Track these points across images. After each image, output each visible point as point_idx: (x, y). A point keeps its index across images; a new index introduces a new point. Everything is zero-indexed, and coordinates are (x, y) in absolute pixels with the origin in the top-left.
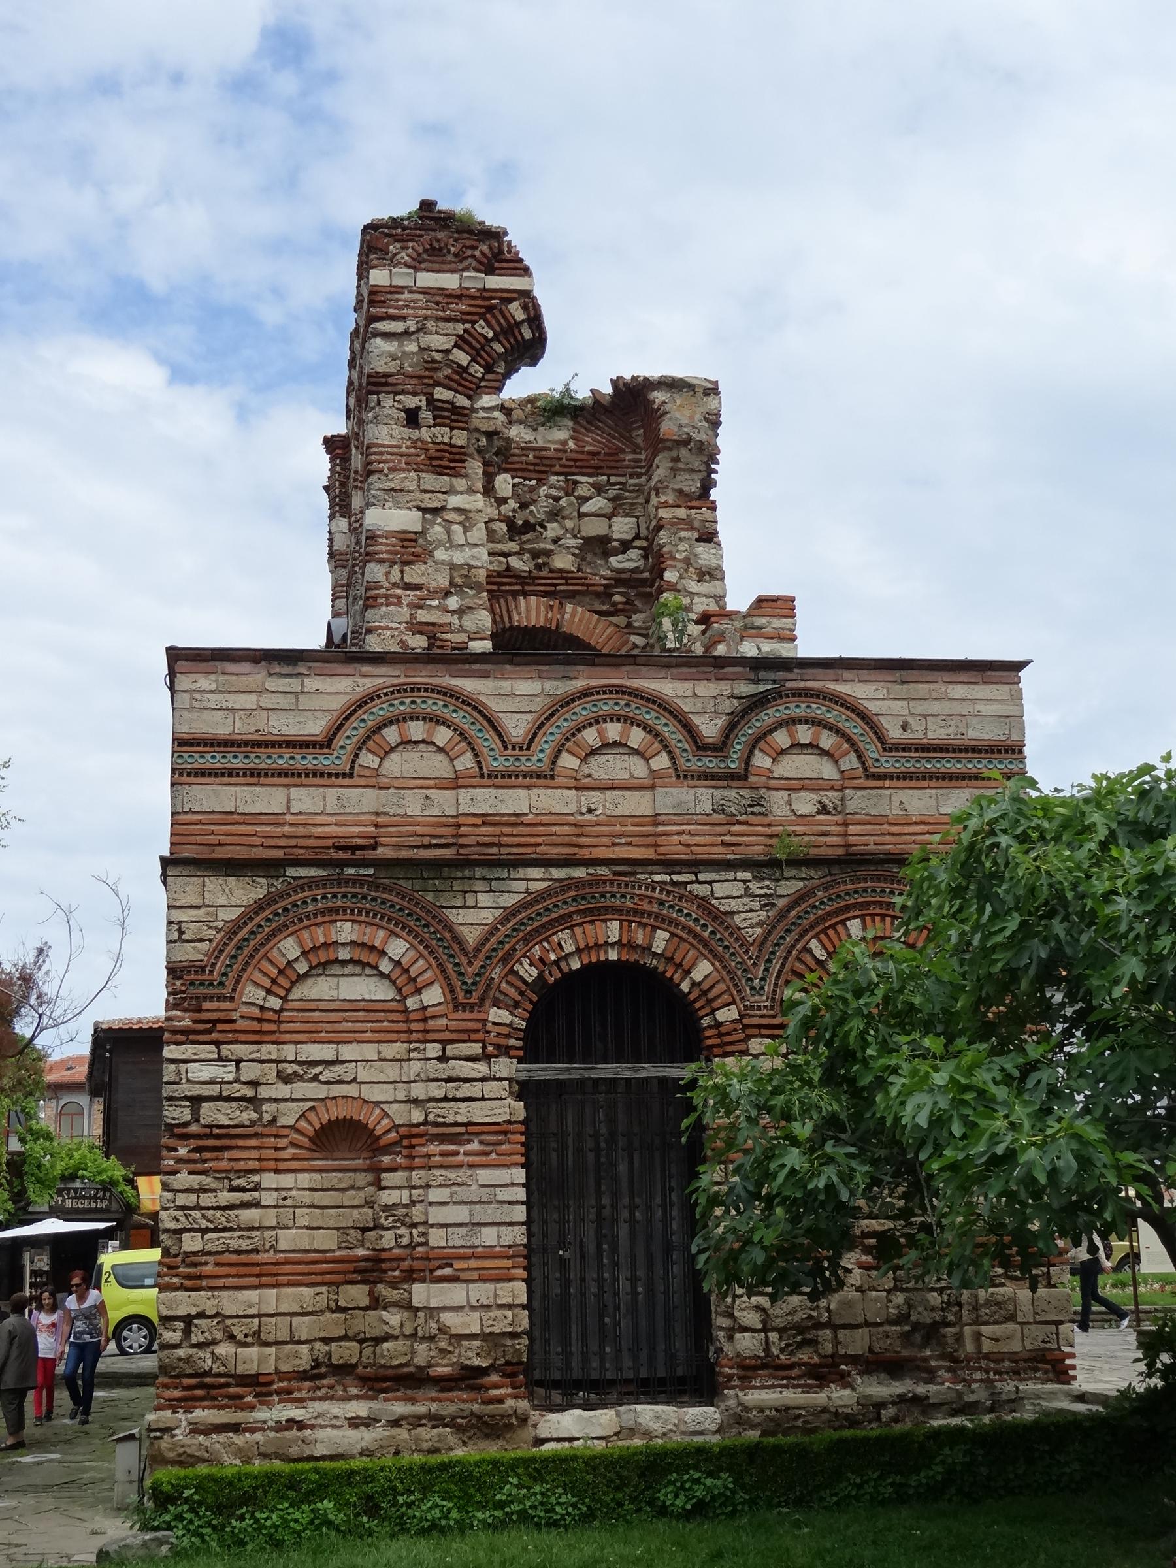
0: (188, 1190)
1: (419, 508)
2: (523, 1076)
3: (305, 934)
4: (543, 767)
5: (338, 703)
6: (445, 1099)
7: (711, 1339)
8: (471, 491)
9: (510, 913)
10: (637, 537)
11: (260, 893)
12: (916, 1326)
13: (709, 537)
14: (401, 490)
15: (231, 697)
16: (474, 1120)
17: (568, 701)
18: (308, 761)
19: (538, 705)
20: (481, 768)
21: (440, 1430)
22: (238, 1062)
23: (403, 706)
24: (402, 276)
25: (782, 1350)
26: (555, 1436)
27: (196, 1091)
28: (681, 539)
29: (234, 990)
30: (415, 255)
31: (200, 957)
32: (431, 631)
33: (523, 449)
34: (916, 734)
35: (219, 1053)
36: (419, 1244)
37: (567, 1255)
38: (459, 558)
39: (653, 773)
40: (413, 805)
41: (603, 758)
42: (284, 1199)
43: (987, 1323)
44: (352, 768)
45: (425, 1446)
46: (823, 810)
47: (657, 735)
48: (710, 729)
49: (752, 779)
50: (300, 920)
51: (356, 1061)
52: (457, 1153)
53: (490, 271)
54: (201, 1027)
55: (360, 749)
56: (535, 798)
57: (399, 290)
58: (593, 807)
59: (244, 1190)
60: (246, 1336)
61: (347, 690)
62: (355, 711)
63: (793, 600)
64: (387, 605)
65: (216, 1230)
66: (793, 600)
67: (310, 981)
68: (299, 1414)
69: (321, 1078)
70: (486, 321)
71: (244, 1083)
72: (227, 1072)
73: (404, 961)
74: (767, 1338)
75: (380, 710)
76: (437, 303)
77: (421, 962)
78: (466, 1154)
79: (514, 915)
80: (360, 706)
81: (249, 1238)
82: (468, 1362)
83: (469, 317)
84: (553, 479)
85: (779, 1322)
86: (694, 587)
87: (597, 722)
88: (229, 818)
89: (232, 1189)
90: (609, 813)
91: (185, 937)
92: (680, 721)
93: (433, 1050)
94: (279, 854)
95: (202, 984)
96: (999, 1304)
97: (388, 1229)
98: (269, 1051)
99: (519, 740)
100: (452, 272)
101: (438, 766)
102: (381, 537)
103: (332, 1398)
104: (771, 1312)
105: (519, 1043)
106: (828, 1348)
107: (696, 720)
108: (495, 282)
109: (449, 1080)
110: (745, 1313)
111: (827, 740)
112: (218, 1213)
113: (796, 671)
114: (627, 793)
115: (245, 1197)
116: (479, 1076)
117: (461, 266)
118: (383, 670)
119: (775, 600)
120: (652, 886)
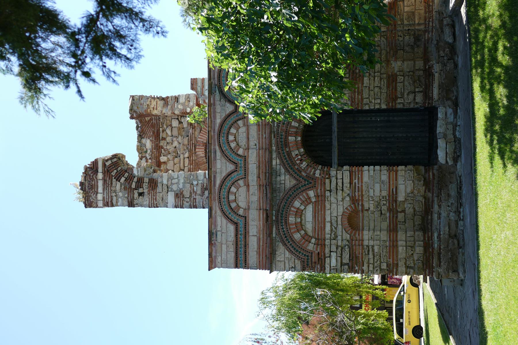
0: (368, 266)
1: (167, 193)
2: (336, 166)
3: (292, 231)
4: (243, 159)
5: (224, 221)
6: (342, 190)
7: (417, 108)
9: (287, 170)
10: (178, 119)
11: (281, 244)
12: (415, 44)
13: (176, 99)
14: (162, 198)
16: (349, 181)
17: (222, 151)
18: (241, 229)
19: (224, 161)
20: (243, 178)
21: (442, 193)
22: (331, 252)
23: (224, 201)
24: (100, 197)
25: (422, 87)
26: (445, 158)
27: (339, 264)
29: (309, 253)
31: (299, 262)
32: (204, 189)
35: (328, 257)
36: (386, 198)
37: (390, 153)
38: (182, 181)
39: (244, 125)
40: (254, 198)
42: (372, 238)
43: (415, 21)
44: (243, 217)
45: (447, 198)
47: (232, 124)
50: (288, 233)
51: (331, 216)
52: (358, 187)
54: (320, 262)
55: (237, 214)
56: (252, 162)
58: (254, 144)
59: (369, 251)
60: (412, 250)
61: (220, 218)
62: (226, 216)
63: (191, 79)
64: (196, 202)
65: (380, 259)
66: (191, 79)
67: (307, 230)
68: (436, 235)
69: (336, 227)
70: (112, 172)
71: (337, 249)
72: (333, 255)
73: (301, 202)
74: (417, 92)
75: (226, 208)
77: (301, 197)
78: (358, 184)
79: (287, 169)
80: (225, 214)
81: (383, 249)
82: (422, 184)
83: (111, 177)
84: (161, 144)
85: (413, 88)
87: (228, 143)
88: (258, 253)
89: (368, 254)
90: (256, 139)
91: (294, 267)
92: (228, 117)
93: (328, 194)
95: (307, 262)
96: (409, 18)
97: (381, 208)
98: (327, 242)
100: (97, 182)
101: (243, 190)
104: (409, 91)
105: (326, 167)
106: (421, 73)
107: (228, 112)
108: (100, 169)
109: (337, 189)
110: (410, 99)
112: (376, 258)
113: (212, 81)
114: (250, 133)
115: (371, 250)
116: (336, 180)
117: (96, 180)
119: (192, 84)
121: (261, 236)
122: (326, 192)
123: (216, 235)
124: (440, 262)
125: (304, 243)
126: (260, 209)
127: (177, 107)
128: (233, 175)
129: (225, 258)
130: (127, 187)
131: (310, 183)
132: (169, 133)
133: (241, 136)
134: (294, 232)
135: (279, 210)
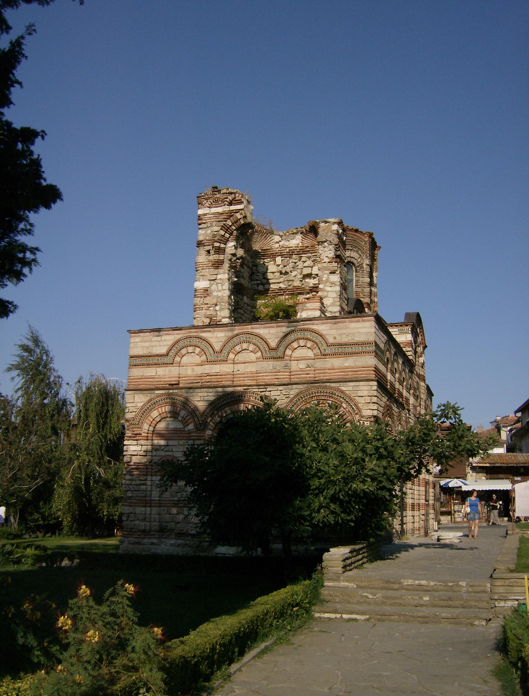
1: (209, 280)
3: (160, 409)
5: (170, 343)
8: (224, 273)
15: (143, 343)
19: (224, 340)
21: (189, 549)
23: (187, 342)
28: (325, 274)
30: (210, 203)
33: (285, 248)
34: (338, 341)
38: (220, 294)
41: (242, 354)
46: (308, 366)
48: (273, 344)
49: (286, 358)
50: (158, 406)
53: (230, 204)
57: (206, 214)
59: (142, 480)
65: (135, 491)
75: (181, 344)
76: (216, 217)
77: (189, 417)
80: (176, 343)
84: (294, 256)
86: (328, 289)
89: (140, 480)
94: (153, 387)
99: (218, 350)
101: (198, 359)
102: (198, 290)
103: (168, 538)
108: (233, 208)
111: (309, 344)
112: (136, 486)
115: (142, 482)
118: (183, 332)
120: (254, 393)
121: (156, 380)
122: (192, 441)
123: (158, 336)
124: (132, 544)
125: (149, 420)
126: (179, 378)
127: (325, 274)
128: (210, 349)
129: (138, 346)
130: (216, 238)
131: (201, 426)
132: (306, 264)
133: (247, 356)
134: (159, 412)
135: (178, 396)
